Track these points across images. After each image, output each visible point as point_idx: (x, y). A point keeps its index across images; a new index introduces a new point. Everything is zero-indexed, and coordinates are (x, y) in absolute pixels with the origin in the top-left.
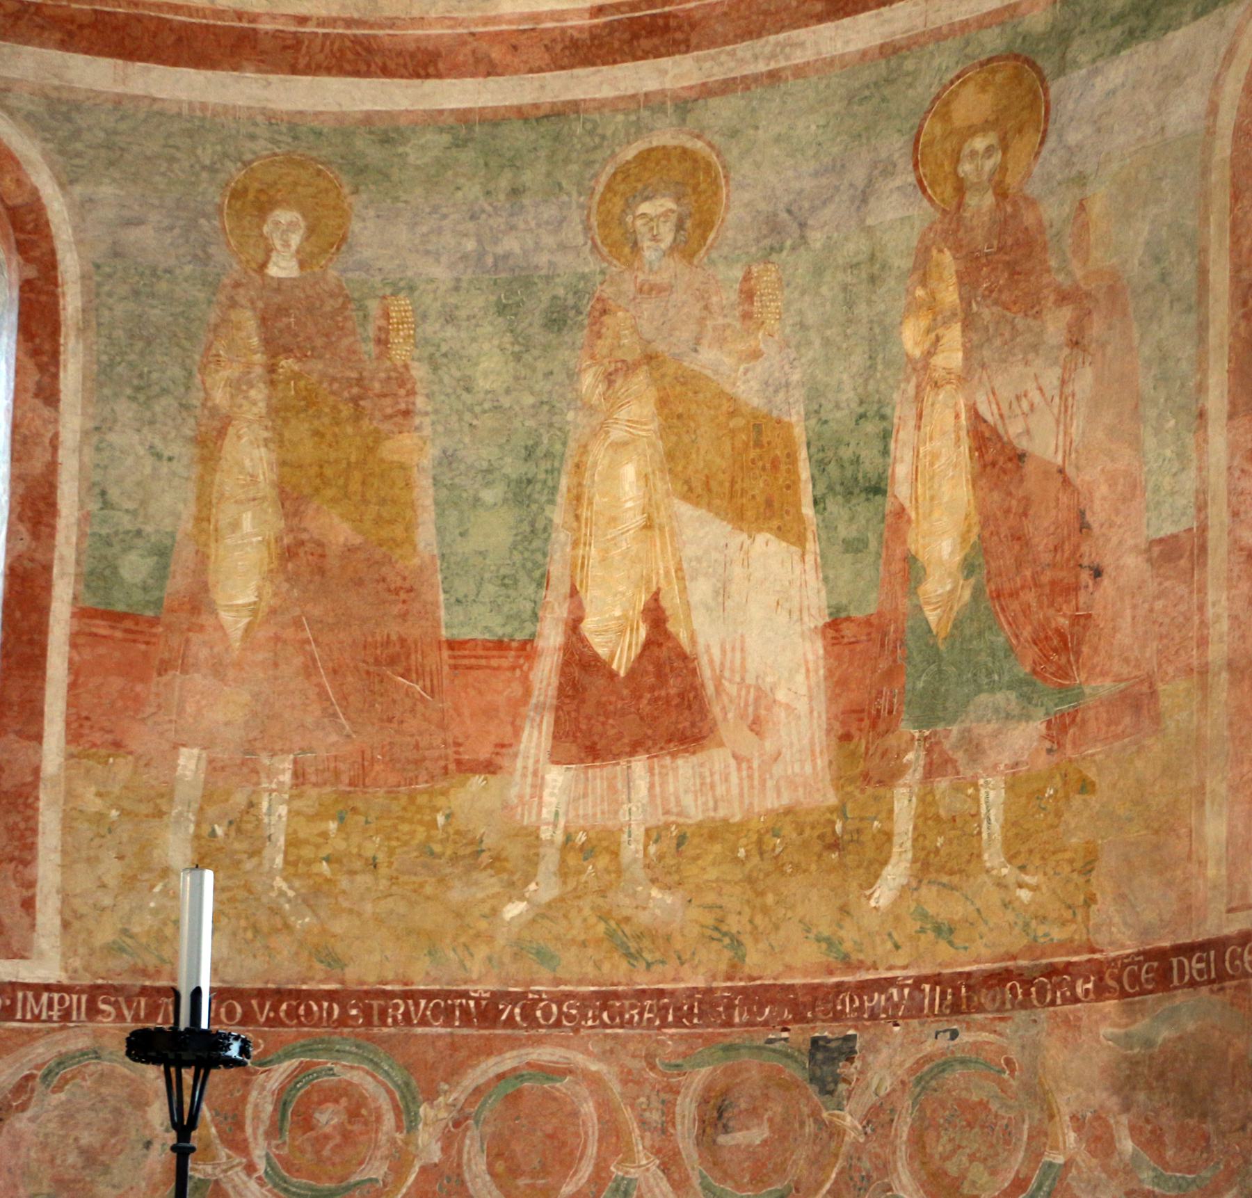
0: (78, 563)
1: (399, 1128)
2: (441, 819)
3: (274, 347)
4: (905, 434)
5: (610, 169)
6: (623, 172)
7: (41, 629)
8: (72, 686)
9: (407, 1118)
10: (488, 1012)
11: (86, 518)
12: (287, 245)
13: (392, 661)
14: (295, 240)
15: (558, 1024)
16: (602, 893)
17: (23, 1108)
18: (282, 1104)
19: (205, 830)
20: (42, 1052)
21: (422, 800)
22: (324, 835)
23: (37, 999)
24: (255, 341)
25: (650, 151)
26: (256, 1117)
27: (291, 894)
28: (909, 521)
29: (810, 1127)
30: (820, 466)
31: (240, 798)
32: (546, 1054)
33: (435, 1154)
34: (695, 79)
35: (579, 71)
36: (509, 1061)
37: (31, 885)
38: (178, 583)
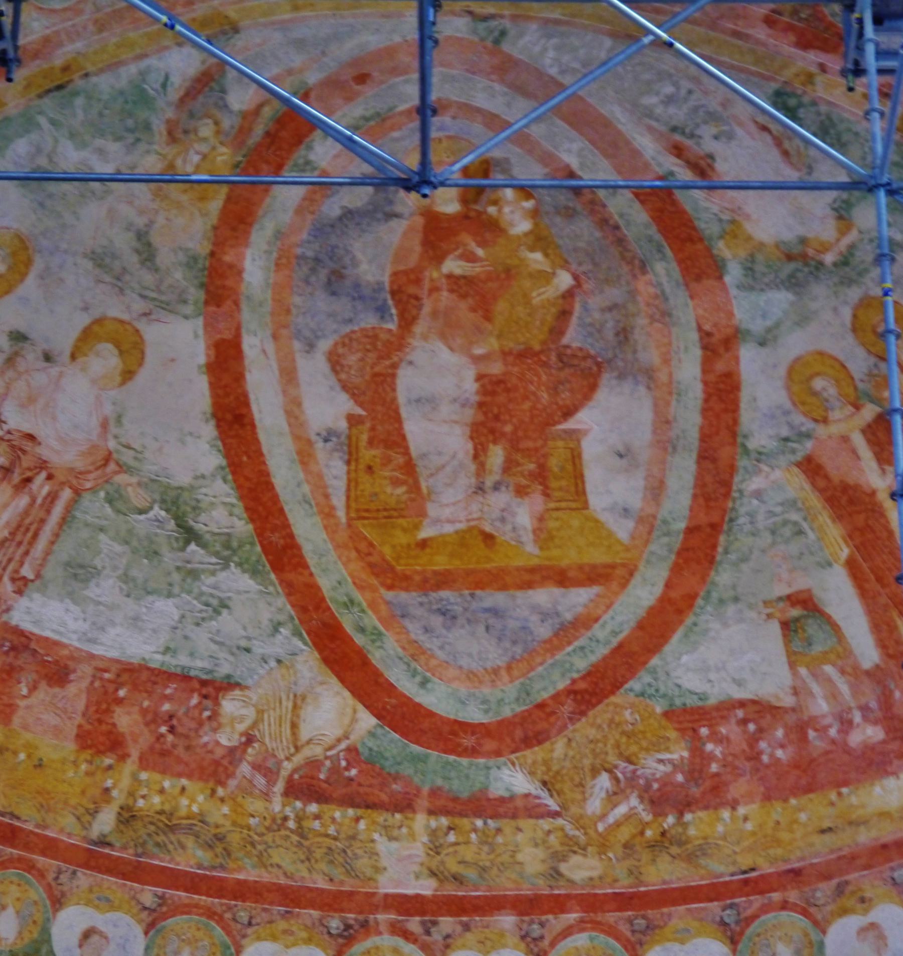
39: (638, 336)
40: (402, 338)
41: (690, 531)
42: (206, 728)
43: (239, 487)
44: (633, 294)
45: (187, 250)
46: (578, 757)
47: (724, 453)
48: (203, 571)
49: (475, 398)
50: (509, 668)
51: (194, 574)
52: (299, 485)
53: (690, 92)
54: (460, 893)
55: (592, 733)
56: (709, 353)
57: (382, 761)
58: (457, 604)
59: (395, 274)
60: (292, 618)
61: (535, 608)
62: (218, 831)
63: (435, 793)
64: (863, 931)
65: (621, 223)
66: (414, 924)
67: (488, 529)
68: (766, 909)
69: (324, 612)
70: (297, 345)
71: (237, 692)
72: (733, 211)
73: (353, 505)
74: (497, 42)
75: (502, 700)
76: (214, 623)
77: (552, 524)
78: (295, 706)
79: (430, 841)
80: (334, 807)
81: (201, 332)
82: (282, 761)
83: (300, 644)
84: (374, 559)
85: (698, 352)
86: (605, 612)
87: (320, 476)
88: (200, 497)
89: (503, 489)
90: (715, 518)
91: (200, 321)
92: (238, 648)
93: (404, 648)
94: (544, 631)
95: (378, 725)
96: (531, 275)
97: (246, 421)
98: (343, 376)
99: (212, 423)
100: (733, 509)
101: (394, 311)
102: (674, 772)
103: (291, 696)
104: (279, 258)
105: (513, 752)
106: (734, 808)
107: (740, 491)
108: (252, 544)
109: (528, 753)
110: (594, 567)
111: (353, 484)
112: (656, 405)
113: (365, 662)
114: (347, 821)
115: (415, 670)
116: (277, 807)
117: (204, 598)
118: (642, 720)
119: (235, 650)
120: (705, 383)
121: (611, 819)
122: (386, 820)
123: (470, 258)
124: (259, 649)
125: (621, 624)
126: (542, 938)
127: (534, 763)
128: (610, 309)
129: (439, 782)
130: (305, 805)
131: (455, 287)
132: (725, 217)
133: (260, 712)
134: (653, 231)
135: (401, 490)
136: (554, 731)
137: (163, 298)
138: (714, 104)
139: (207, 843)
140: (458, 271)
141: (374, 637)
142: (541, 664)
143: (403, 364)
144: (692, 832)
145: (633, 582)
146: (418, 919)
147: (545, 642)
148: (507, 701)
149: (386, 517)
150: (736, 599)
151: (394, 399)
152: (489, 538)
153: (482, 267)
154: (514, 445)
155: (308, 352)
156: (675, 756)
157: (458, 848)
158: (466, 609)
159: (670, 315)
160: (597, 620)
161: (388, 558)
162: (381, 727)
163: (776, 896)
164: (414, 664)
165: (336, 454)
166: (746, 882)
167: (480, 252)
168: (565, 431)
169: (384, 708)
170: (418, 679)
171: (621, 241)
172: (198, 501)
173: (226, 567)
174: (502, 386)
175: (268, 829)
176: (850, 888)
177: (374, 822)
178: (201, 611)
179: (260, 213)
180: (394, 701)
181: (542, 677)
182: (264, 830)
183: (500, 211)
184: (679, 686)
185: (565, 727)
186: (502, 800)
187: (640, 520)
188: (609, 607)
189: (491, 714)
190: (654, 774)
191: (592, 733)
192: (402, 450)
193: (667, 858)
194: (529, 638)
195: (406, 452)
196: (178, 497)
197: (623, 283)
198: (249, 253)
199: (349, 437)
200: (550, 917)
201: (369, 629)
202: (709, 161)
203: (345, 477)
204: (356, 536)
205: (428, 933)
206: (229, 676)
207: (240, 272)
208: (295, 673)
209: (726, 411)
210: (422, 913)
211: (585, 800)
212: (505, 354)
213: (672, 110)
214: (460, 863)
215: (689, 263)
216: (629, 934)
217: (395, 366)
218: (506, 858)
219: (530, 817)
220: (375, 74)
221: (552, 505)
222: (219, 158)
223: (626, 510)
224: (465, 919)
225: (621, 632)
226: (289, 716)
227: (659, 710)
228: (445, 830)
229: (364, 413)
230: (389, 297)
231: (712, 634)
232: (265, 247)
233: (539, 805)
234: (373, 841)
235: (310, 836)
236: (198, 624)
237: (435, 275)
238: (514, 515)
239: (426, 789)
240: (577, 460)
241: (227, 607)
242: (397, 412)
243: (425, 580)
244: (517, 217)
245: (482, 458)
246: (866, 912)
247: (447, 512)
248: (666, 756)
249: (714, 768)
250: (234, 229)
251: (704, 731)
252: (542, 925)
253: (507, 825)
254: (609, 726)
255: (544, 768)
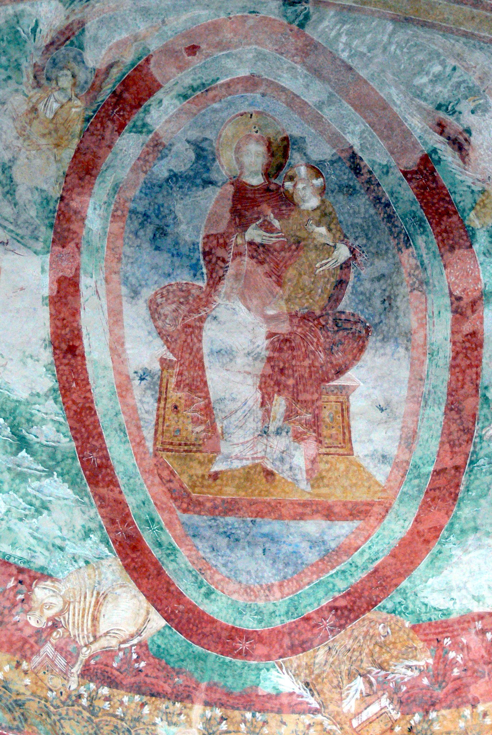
39: (399, 302)
40: (209, 295)
41: (437, 473)
42: (18, 609)
43: (68, 409)
44: (398, 265)
45: (42, 191)
46: (337, 663)
47: (469, 403)
48: (31, 475)
49: (266, 353)
50: (281, 585)
51: (23, 477)
52: (116, 415)
53: (454, 69)
55: (349, 643)
56: (458, 316)
57: (168, 657)
58: (240, 529)
59: (207, 237)
60: (101, 527)
61: (305, 536)
62: (19, 697)
63: (211, 687)
65: (391, 200)
67: (269, 467)
69: (128, 526)
70: (124, 290)
71: (49, 583)
72: (483, 181)
73: (160, 438)
74: (301, 26)
75: (274, 612)
76: (34, 520)
77: (322, 466)
78: (97, 602)
79: (205, 728)
80: (123, 692)
81: (47, 268)
82: (81, 647)
83: (106, 550)
84: (174, 485)
85: (448, 316)
86: (364, 543)
87: (135, 409)
88: (33, 411)
89: (284, 434)
90: (458, 461)
91: (47, 258)
92: (53, 545)
93: (193, 563)
94: (312, 557)
95: (166, 626)
96: (316, 247)
97: (77, 352)
98: (160, 323)
99: (50, 349)
100: (474, 452)
101: (204, 270)
102: (420, 676)
103: (95, 593)
104: (116, 210)
105: (281, 657)
106: (474, 706)
107: (481, 437)
108: (73, 458)
109: (293, 658)
110: (356, 504)
111: (161, 420)
112: (412, 365)
113: (160, 572)
114: (133, 705)
115: (202, 582)
116: (74, 686)
117: (29, 498)
118: (392, 633)
119: (50, 547)
120: (454, 343)
121: (364, 716)
122: (167, 708)
123: (268, 228)
124: (71, 549)
125: (377, 553)
127: (299, 666)
128: (379, 279)
129: (216, 679)
130: (98, 688)
131: (255, 254)
132: (476, 188)
133: (67, 603)
134: (417, 208)
135: (200, 428)
136: (317, 641)
137: (19, 231)
138: (473, 80)
139: (7, 706)
140: (258, 240)
141: (168, 551)
142: (309, 584)
143: (209, 319)
144: (436, 727)
145: (388, 517)
147: (312, 565)
148: (277, 613)
149: (185, 451)
150: (476, 529)
151: (200, 349)
152: (269, 474)
153: (277, 237)
154: (295, 398)
155: (133, 298)
156: (422, 663)
158: (247, 534)
159: (427, 284)
160: (356, 549)
161: (185, 485)
162: (170, 628)
164: (200, 577)
165: (149, 392)
167: (277, 224)
168: (336, 387)
169: (173, 612)
170: (203, 590)
171: (390, 217)
172: (32, 415)
173: (49, 475)
174: (288, 344)
175: (63, 703)
177: (157, 709)
178: (25, 509)
179: (103, 167)
180: (181, 607)
181: (308, 595)
182: (59, 704)
183: (295, 186)
184: (426, 605)
185: (327, 637)
186: (269, 697)
187: (396, 465)
188: (367, 539)
189: (263, 624)
190: (403, 679)
191: (349, 643)
192: (203, 394)
194: (299, 561)
195: (207, 397)
196: (15, 409)
197: (390, 256)
198: (92, 202)
199: (161, 379)
201: (166, 544)
202: (466, 135)
203: (155, 413)
204: (160, 465)
206: (42, 568)
207: (83, 219)
208: (100, 574)
209: (470, 366)
211: (342, 699)
212: (292, 316)
213: (438, 89)
215: (445, 235)
217: (202, 320)
219: (293, 712)
220: (203, 46)
221: (324, 450)
222: (74, 110)
223: (384, 457)
225: (377, 559)
226: (91, 610)
227: (407, 624)
228: (218, 720)
229: (175, 359)
230: (201, 257)
231: (455, 559)
232: (105, 199)
233: (301, 703)
234: (155, 724)
235: (100, 714)
236: (21, 520)
237: (240, 241)
238: (292, 457)
239: (203, 685)
240: (345, 413)
241: (47, 508)
242: (201, 360)
243: (215, 507)
244: (308, 192)
245: (268, 406)
247: (237, 450)
248: (413, 663)
249: (456, 672)
250: (81, 179)
251: (447, 642)
253: (273, 718)
254: (364, 637)
255: (307, 671)
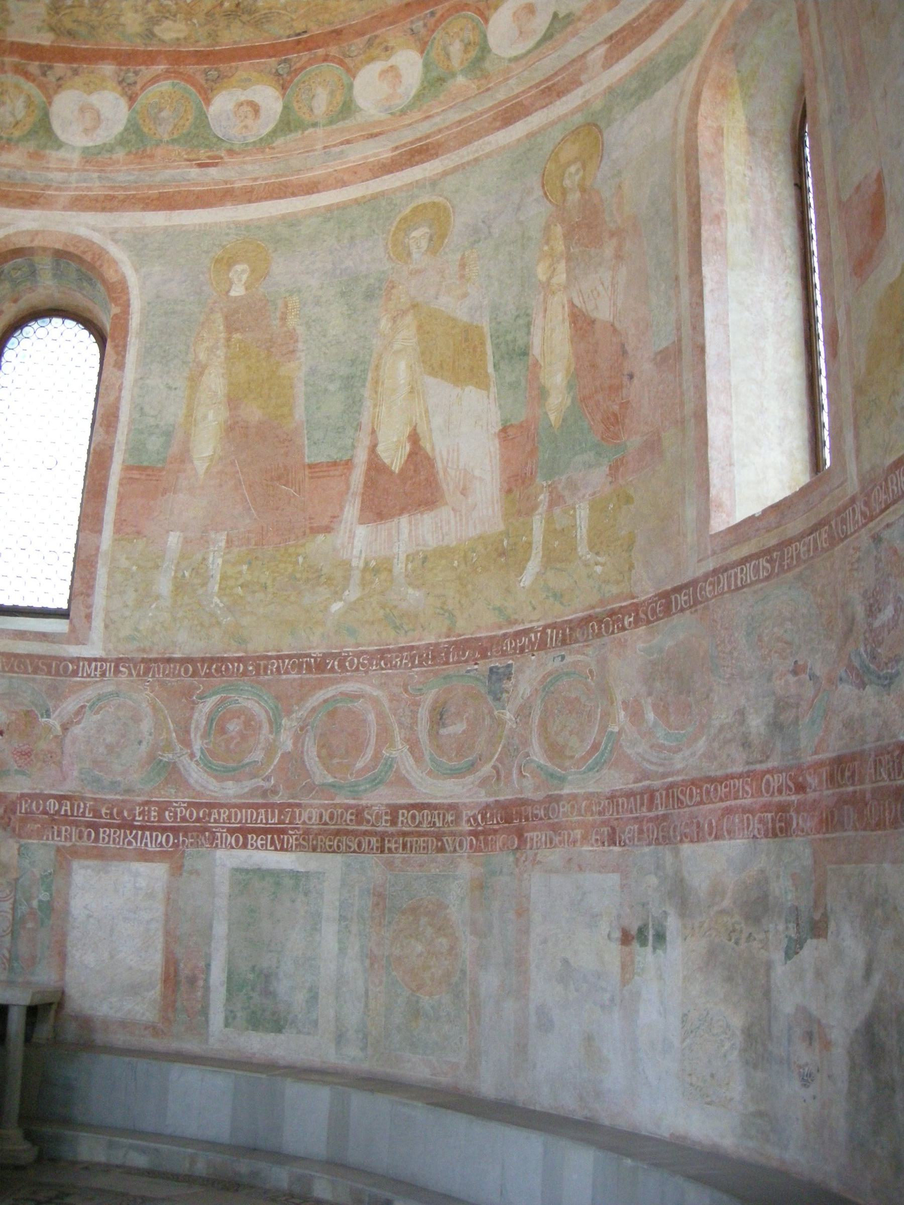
0: (127, 443)
1: (271, 732)
2: (301, 560)
3: (230, 328)
4: (538, 321)
5: (398, 219)
6: (405, 219)
7: (106, 478)
8: (119, 505)
9: (275, 726)
10: (320, 665)
11: (132, 421)
12: (240, 280)
13: (279, 478)
14: (244, 277)
15: (357, 669)
16: (382, 593)
17: (79, 722)
18: (210, 720)
19: (179, 575)
20: (90, 693)
21: (291, 550)
22: (240, 573)
23: (90, 666)
24: (221, 328)
25: (417, 207)
26: (197, 727)
27: (221, 605)
28: (541, 367)
29: (488, 721)
30: (497, 346)
31: (199, 556)
32: (350, 687)
33: (289, 746)
34: (440, 170)
35: (386, 177)
36: (330, 692)
37: (90, 607)
38: (175, 449)
54: (73, 46)
64: (383, 73)
66: (34, 67)
68: (310, 62)
126: (135, 83)
146: (37, 63)
157: (74, 10)
163: (321, 52)
166: (298, 42)
176: (378, 41)
193: (239, 24)
200: (143, 67)
205: (44, 74)
210: (41, 59)
214: (74, 21)
216: (203, 82)
218: (111, 20)
224: (75, 65)
246: (389, 57)
252: (136, 73)
